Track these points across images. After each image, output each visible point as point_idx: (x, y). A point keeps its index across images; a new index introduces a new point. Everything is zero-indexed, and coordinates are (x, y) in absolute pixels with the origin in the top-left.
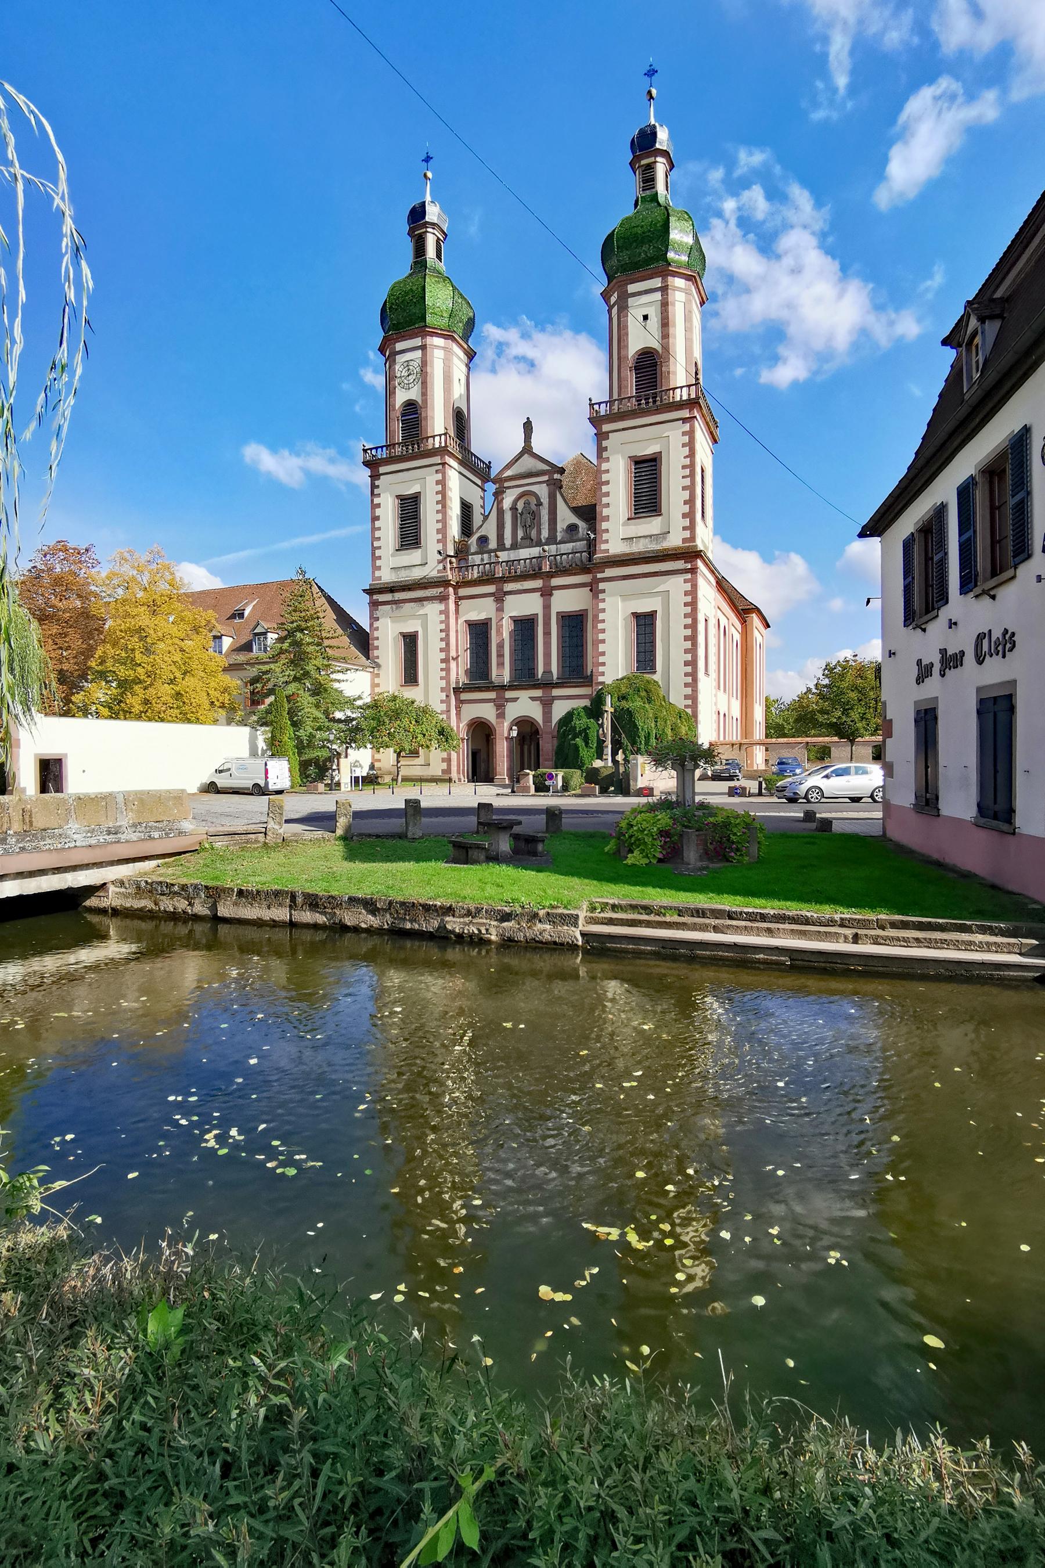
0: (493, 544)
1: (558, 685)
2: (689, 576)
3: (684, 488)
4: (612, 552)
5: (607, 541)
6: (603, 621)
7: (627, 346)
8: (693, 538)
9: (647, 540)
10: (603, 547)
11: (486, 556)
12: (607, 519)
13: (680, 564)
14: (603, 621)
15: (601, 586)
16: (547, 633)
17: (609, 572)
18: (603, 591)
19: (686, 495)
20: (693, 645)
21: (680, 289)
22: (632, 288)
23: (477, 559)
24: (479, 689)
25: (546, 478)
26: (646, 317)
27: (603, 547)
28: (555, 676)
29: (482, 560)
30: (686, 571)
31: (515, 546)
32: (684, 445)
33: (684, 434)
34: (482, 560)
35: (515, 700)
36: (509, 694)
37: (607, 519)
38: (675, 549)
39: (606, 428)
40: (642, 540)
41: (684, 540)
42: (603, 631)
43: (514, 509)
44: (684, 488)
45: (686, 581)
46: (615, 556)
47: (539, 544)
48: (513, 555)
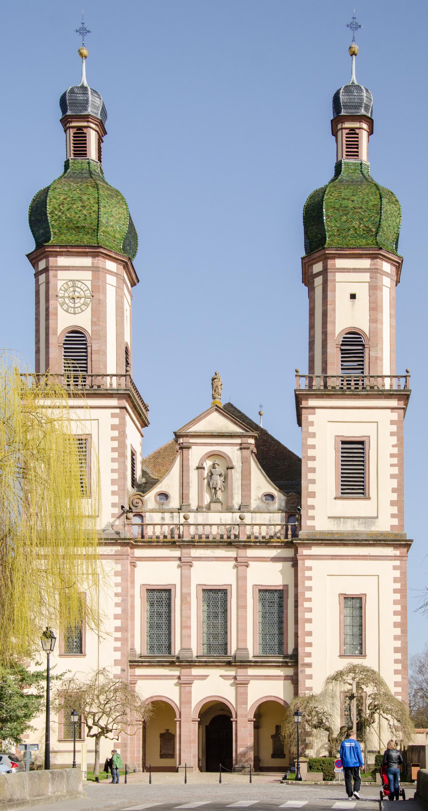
0: (174, 503)
1: (256, 664)
2: (398, 563)
3: (392, 476)
4: (317, 529)
5: (313, 518)
6: (310, 600)
7: (334, 323)
8: (401, 526)
9: (356, 523)
10: (309, 523)
11: (167, 515)
12: (313, 495)
13: (389, 551)
14: (310, 600)
15: (308, 563)
16: (242, 607)
17: (316, 550)
18: (310, 569)
19: (394, 483)
20: (402, 631)
21: (387, 274)
22: (340, 263)
23: (156, 518)
24: (161, 664)
25: (239, 441)
26: (353, 296)
27: (309, 523)
28: (251, 655)
29: (163, 518)
30: (395, 558)
31: (199, 510)
32: (392, 434)
33: (392, 422)
34: (163, 518)
35: (204, 677)
36: (195, 671)
37: (313, 495)
38: (382, 534)
39: (312, 403)
40: (349, 521)
41: (392, 526)
42: (310, 610)
43: (200, 468)
44: (392, 476)
45: (395, 568)
46: (322, 533)
47: (229, 510)
48: (200, 518)
